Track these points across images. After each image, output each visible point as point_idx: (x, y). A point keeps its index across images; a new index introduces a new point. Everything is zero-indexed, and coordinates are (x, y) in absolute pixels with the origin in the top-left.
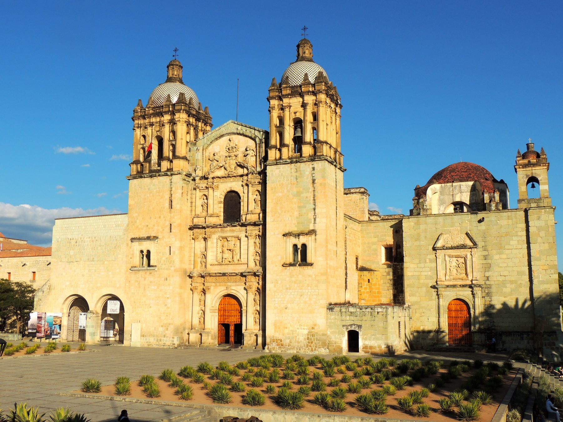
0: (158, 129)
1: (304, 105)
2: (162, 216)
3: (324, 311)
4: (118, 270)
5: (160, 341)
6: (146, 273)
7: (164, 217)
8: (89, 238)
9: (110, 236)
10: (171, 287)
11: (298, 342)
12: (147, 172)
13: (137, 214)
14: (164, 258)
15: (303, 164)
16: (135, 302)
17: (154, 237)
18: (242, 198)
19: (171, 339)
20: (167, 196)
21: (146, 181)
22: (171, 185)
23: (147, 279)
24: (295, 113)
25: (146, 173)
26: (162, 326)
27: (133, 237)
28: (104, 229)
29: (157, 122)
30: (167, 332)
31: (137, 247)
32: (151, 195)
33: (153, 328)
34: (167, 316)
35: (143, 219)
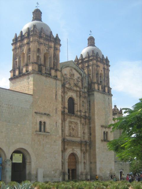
0: (47, 49)
1: (104, 68)
2: (52, 103)
3: (113, 163)
4: (27, 132)
5: (53, 180)
6: (44, 136)
7: (53, 104)
8: (6, 105)
9: (22, 108)
10: (57, 147)
11: (107, 177)
12: (44, 73)
13: (38, 97)
14: (54, 129)
15: (106, 96)
16: (38, 155)
17: (48, 114)
18: (76, 103)
19: (58, 178)
20: (54, 92)
21: (43, 78)
22: (56, 85)
23: (45, 140)
24: (101, 71)
25: (43, 73)
26: (53, 171)
27: (36, 111)
28: (17, 101)
29: (47, 45)
30: (56, 174)
31: (39, 119)
32: (46, 87)
33: (49, 172)
34: (56, 164)
35: (41, 101)
